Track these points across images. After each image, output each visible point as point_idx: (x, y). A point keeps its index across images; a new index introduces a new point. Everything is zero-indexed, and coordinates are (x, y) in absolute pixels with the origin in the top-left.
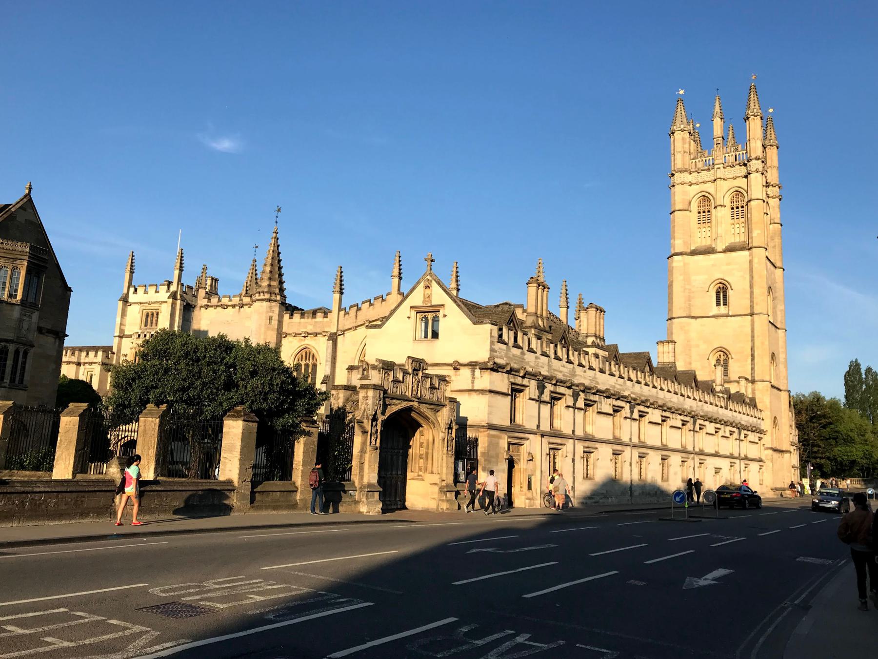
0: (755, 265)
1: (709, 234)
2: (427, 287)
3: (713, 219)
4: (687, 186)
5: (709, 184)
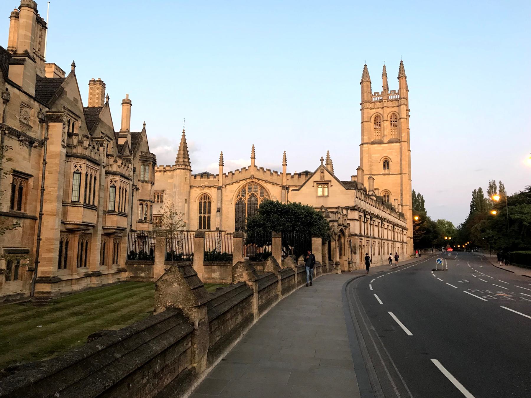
0: (403, 150)
1: (380, 134)
3: (382, 127)
4: (369, 110)
5: (380, 109)
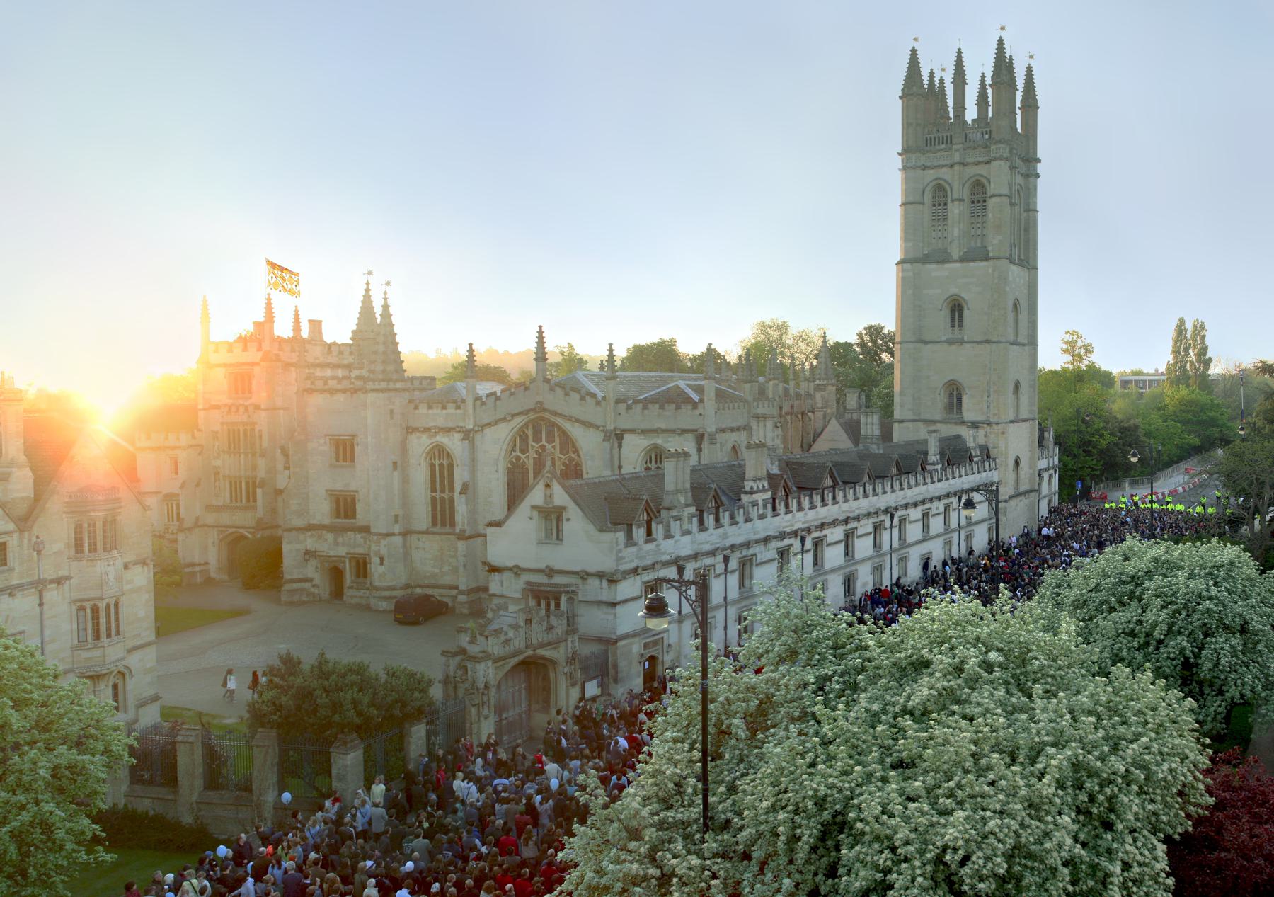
2: (547, 486)
5: (944, 170)
